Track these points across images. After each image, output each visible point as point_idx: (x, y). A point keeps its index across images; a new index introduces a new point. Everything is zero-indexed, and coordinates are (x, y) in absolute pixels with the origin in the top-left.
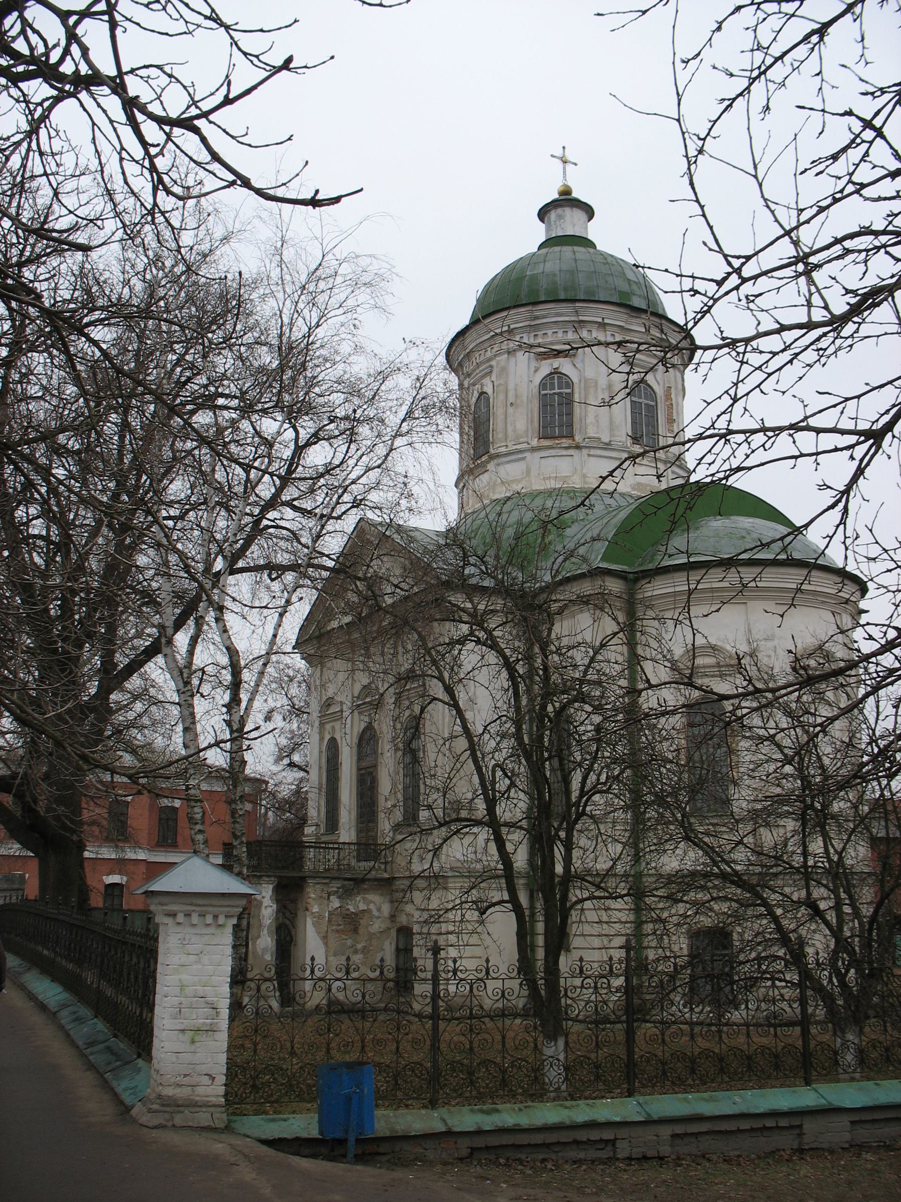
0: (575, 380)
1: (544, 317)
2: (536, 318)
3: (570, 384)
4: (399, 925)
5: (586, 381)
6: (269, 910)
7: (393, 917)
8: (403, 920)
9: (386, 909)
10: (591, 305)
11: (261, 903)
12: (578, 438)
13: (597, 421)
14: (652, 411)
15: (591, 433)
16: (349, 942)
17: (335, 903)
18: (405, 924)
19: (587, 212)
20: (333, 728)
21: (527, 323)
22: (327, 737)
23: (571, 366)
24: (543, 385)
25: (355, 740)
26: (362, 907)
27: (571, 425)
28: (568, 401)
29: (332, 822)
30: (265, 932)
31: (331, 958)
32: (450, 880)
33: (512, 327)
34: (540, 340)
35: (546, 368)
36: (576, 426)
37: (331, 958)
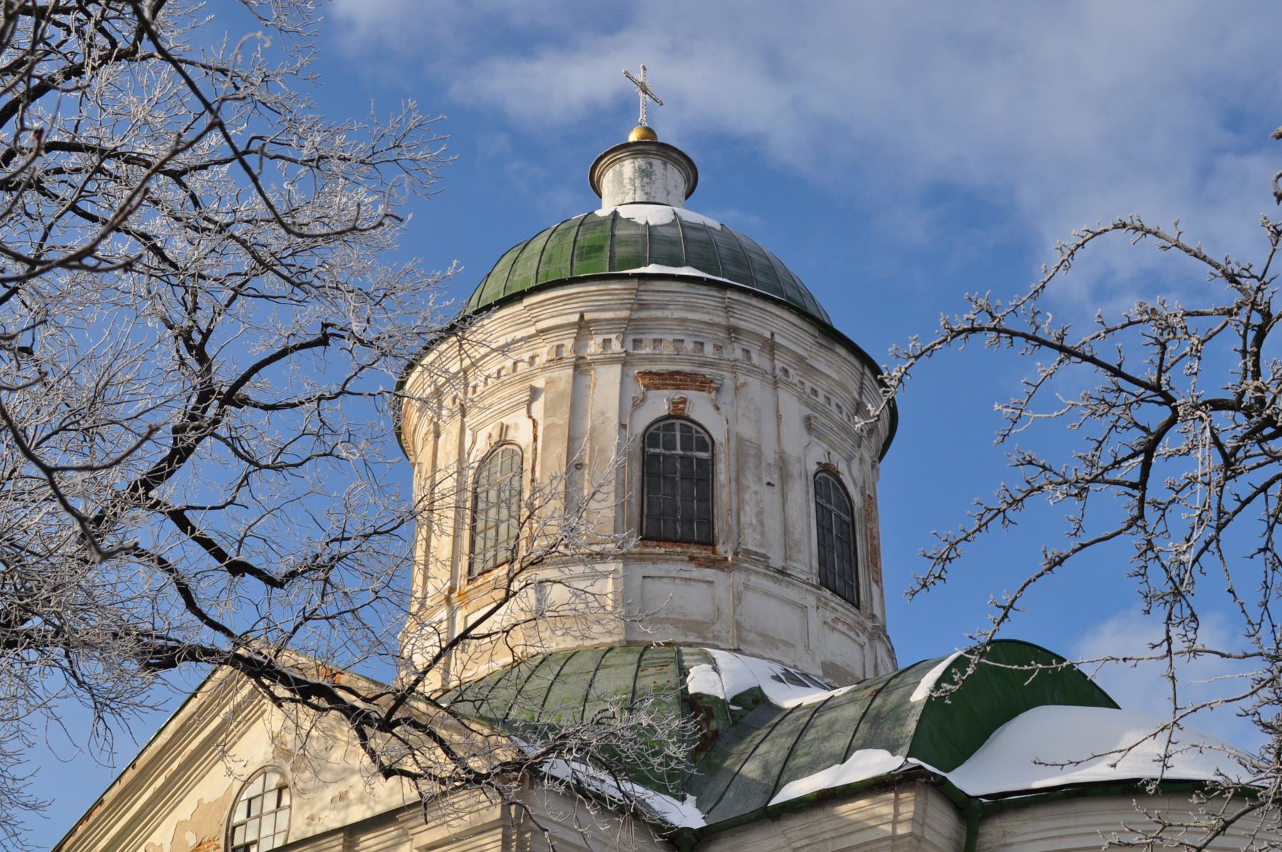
0: (718, 434)
1: (662, 306)
2: (643, 306)
3: (706, 443)
5: (741, 441)
10: (754, 302)
12: (724, 549)
13: (762, 524)
14: (849, 529)
15: (751, 541)
19: (687, 180)
21: (625, 314)
23: (711, 410)
24: (650, 437)
27: (707, 521)
28: (703, 475)
33: (587, 317)
34: (647, 350)
35: (659, 404)
36: (719, 526)
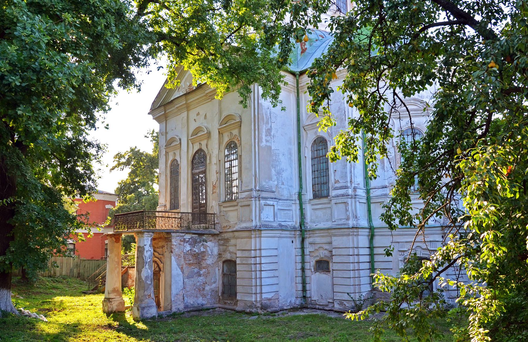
4: (224, 259)
6: (149, 253)
7: (220, 255)
8: (228, 256)
9: (216, 251)
11: (144, 249)
16: (196, 270)
17: (188, 248)
18: (229, 258)
20: (175, 153)
22: (171, 158)
25: (190, 159)
26: (202, 249)
29: (175, 204)
30: (147, 266)
31: (186, 280)
32: (262, 232)
37: (186, 280)
